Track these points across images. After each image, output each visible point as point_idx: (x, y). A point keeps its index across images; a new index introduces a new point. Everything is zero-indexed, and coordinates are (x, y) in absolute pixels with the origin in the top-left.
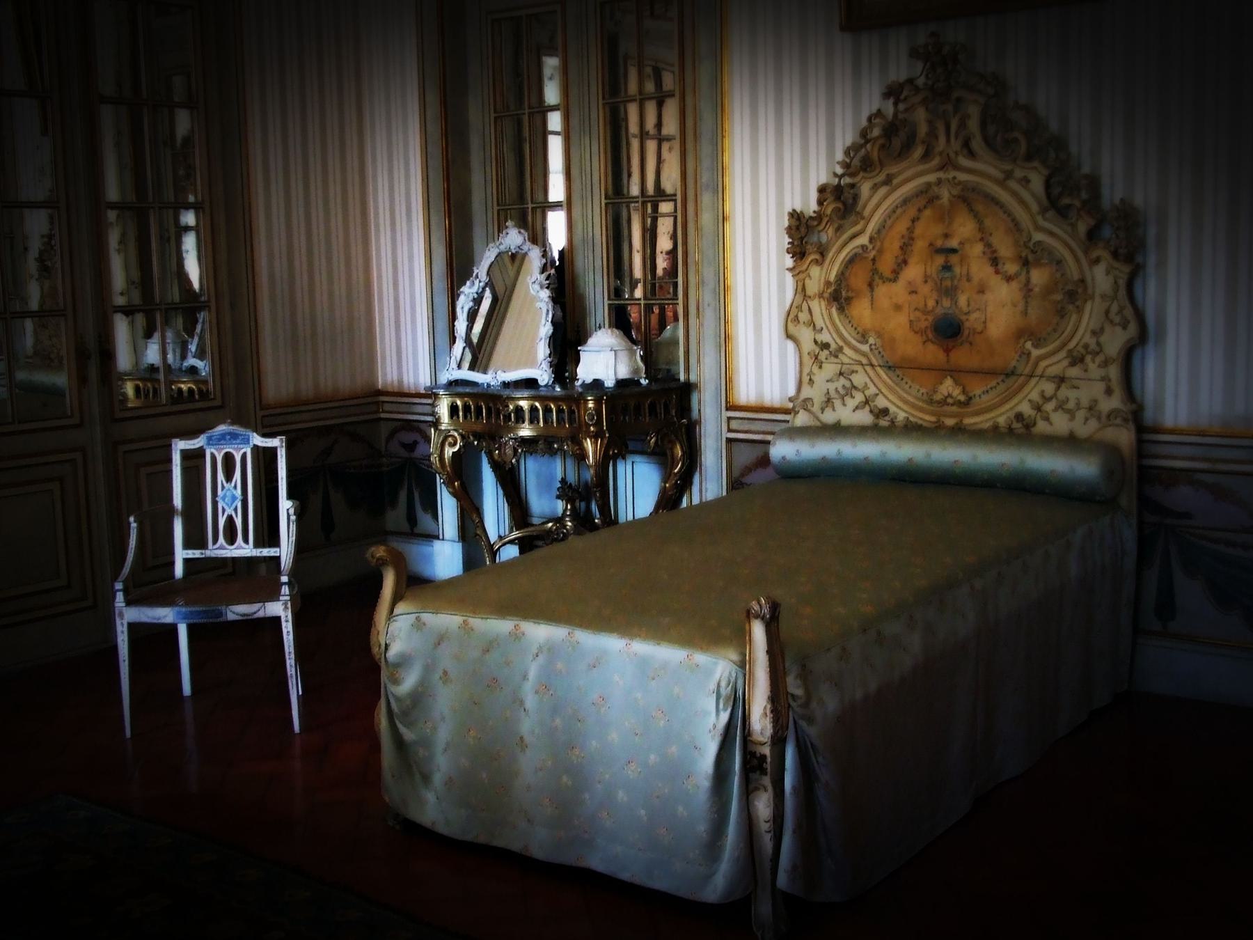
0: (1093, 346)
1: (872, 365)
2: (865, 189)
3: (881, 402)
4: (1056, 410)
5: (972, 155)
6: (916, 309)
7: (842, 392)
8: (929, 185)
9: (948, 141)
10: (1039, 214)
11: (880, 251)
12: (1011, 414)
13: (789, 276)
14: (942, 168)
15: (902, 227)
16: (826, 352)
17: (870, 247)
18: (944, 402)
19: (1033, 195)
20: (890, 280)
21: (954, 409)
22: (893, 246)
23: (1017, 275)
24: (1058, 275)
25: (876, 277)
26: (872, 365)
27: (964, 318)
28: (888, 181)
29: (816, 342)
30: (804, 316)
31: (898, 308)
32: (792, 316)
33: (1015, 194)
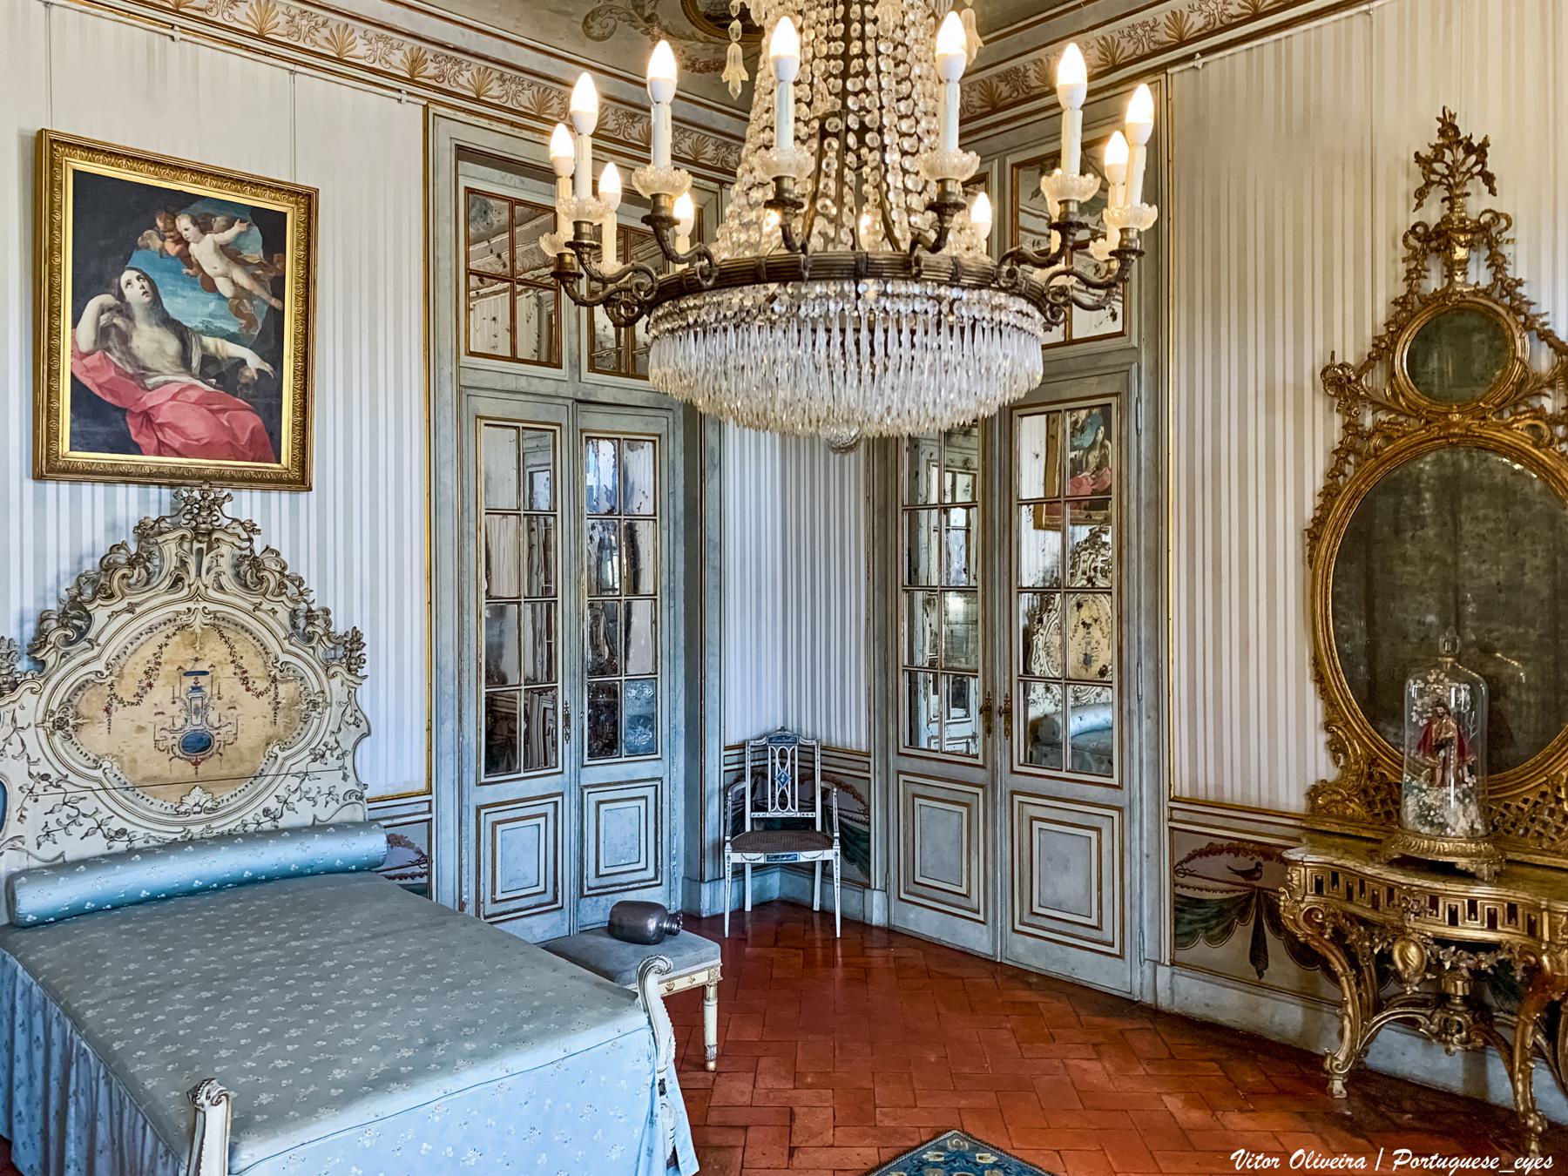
0: (332, 744)
1: (105, 789)
2: (100, 614)
3: (116, 824)
5: (221, 588)
8: (178, 613)
9: (199, 574)
11: (120, 676)
15: (148, 651)
19: (281, 624)
21: (203, 815)
22: (135, 668)
23: (267, 690)
24: (302, 689)
25: (115, 703)
26: (105, 789)
27: (214, 732)
28: (131, 609)
29: (30, 774)
31: (141, 729)
33: (263, 623)
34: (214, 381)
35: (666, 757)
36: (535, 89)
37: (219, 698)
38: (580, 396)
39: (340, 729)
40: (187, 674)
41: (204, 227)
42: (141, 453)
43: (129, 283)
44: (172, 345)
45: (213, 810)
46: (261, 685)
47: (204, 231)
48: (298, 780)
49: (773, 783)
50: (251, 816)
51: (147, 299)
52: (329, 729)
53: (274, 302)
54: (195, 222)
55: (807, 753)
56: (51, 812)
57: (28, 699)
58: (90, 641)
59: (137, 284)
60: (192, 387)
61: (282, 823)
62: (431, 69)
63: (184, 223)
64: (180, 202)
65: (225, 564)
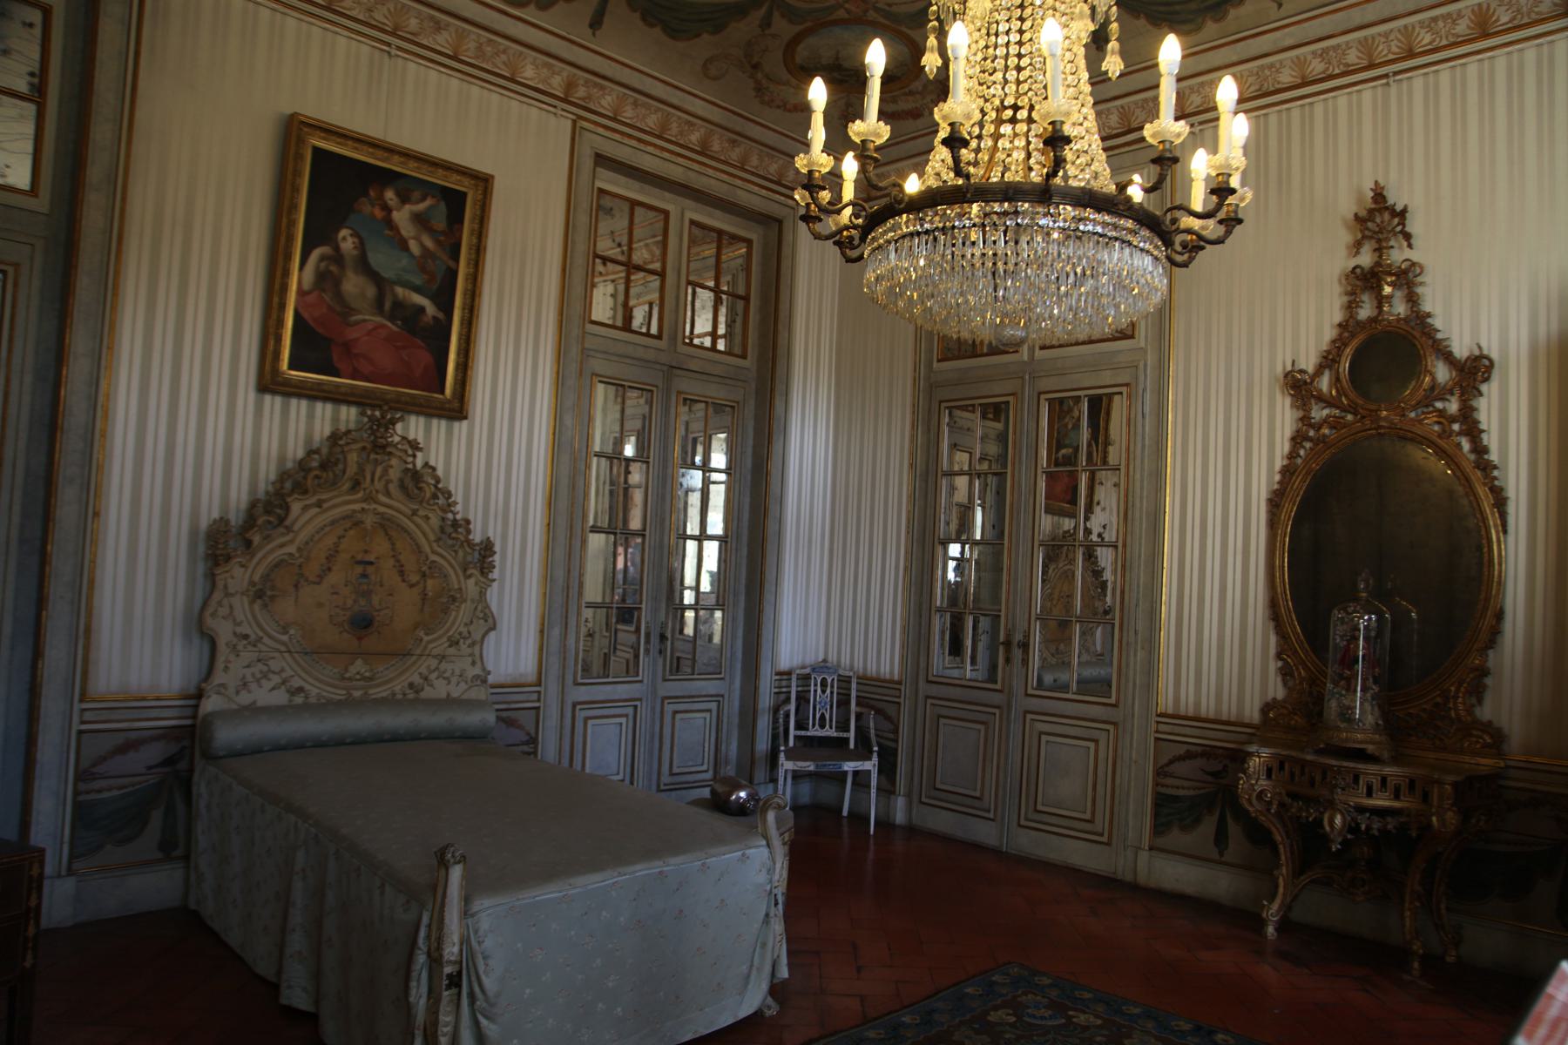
1: (289, 652)
2: (296, 508)
3: (296, 683)
5: (388, 494)
6: (337, 607)
7: (258, 676)
8: (354, 511)
9: (372, 480)
10: (435, 541)
12: (406, 684)
14: (364, 500)
15: (330, 541)
17: (297, 555)
19: (433, 530)
20: (314, 583)
21: (362, 683)
23: (418, 583)
27: (375, 614)
28: (319, 504)
29: (235, 633)
31: (320, 605)
33: (418, 526)
34: (399, 322)
35: (727, 678)
36: (660, 114)
37: (381, 586)
38: (674, 364)
39: (472, 622)
41: (404, 199)
43: (344, 239)
44: (371, 291)
45: (371, 679)
46: (414, 578)
48: (436, 662)
50: (398, 686)
51: (355, 252)
52: (464, 620)
53: (451, 264)
54: (398, 194)
55: (845, 681)
56: (248, 666)
57: (238, 572)
58: (286, 527)
59: (350, 240)
60: (383, 326)
61: (423, 695)
62: (581, 92)
64: (390, 177)
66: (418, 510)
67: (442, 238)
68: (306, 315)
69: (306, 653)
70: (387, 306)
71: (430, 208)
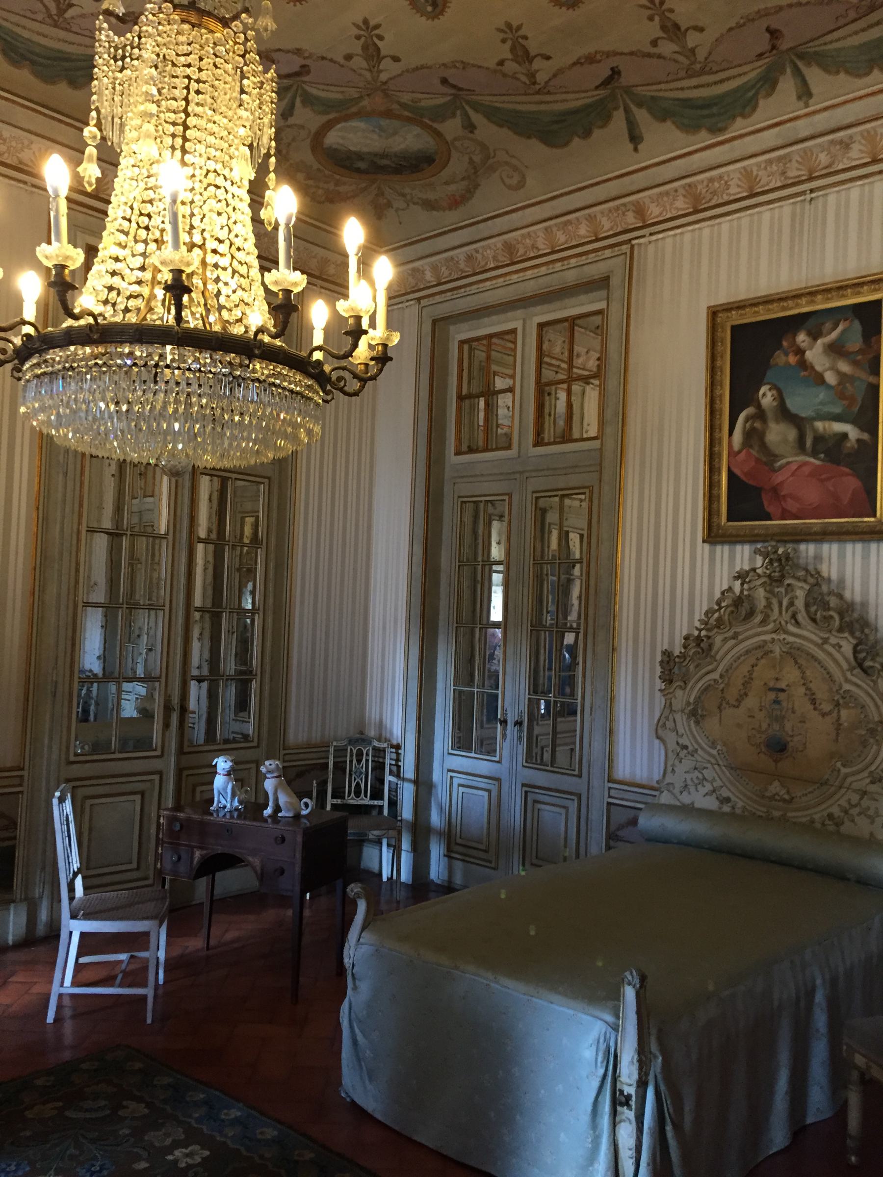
1: (719, 765)
2: (718, 640)
3: (725, 793)
4: (860, 814)
5: (797, 624)
6: (753, 729)
8: (765, 642)
9: (780, 613)
10: (848, 670)
11: (728, 685)
12: (825, 814)
13: (658, 694)
15: (744, 669)
16: (685, 751)
18: (772, 798)
21: (781, 804)
23: (830, 713)
24: (862, 716)
25: (724, 704)
26: (719, 765)
27: (789, 739)
28: (735, 636)
29: (678, 743)
30: (670, 724)
31: (739, 726)
32: (661, 723)
33: (830, 654)
40: (771, 689)
41: (815, 336)
42: (771, 519)
43: (764, 395)
44: (792, 434)
46: (826, 707)
47: (815, 339)
48: (857, 797)
49: (350, 775)
51: (775, 404)
53: (871, 379)
54: (809, 334)
60: (806, 464)
63: (802, 338)
65: (800, 603)
66: (828, 638)
67: (859, 357)
68: (737, 471)
69: (732, 768)
70: (809, 443)
71: (843, 332)
